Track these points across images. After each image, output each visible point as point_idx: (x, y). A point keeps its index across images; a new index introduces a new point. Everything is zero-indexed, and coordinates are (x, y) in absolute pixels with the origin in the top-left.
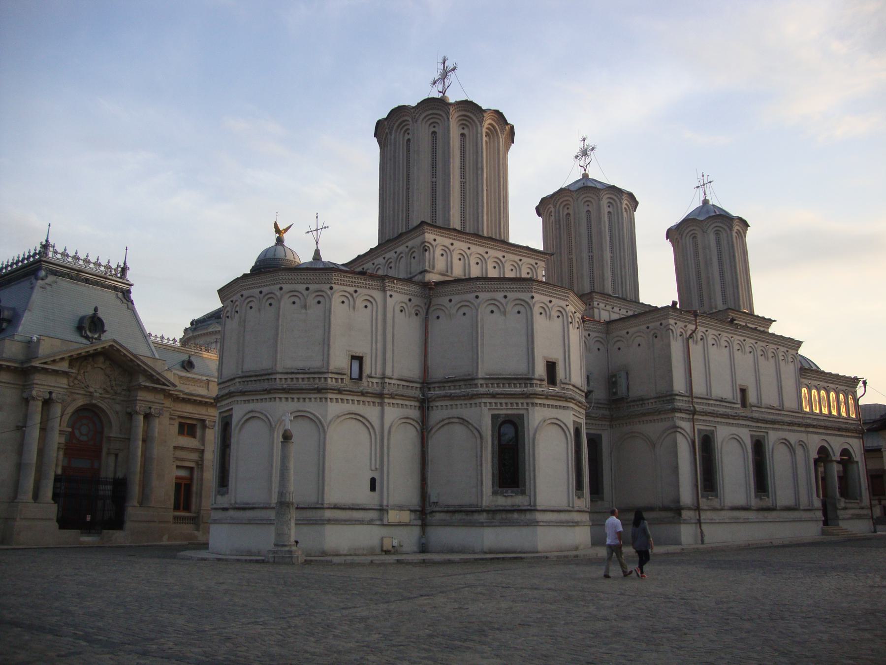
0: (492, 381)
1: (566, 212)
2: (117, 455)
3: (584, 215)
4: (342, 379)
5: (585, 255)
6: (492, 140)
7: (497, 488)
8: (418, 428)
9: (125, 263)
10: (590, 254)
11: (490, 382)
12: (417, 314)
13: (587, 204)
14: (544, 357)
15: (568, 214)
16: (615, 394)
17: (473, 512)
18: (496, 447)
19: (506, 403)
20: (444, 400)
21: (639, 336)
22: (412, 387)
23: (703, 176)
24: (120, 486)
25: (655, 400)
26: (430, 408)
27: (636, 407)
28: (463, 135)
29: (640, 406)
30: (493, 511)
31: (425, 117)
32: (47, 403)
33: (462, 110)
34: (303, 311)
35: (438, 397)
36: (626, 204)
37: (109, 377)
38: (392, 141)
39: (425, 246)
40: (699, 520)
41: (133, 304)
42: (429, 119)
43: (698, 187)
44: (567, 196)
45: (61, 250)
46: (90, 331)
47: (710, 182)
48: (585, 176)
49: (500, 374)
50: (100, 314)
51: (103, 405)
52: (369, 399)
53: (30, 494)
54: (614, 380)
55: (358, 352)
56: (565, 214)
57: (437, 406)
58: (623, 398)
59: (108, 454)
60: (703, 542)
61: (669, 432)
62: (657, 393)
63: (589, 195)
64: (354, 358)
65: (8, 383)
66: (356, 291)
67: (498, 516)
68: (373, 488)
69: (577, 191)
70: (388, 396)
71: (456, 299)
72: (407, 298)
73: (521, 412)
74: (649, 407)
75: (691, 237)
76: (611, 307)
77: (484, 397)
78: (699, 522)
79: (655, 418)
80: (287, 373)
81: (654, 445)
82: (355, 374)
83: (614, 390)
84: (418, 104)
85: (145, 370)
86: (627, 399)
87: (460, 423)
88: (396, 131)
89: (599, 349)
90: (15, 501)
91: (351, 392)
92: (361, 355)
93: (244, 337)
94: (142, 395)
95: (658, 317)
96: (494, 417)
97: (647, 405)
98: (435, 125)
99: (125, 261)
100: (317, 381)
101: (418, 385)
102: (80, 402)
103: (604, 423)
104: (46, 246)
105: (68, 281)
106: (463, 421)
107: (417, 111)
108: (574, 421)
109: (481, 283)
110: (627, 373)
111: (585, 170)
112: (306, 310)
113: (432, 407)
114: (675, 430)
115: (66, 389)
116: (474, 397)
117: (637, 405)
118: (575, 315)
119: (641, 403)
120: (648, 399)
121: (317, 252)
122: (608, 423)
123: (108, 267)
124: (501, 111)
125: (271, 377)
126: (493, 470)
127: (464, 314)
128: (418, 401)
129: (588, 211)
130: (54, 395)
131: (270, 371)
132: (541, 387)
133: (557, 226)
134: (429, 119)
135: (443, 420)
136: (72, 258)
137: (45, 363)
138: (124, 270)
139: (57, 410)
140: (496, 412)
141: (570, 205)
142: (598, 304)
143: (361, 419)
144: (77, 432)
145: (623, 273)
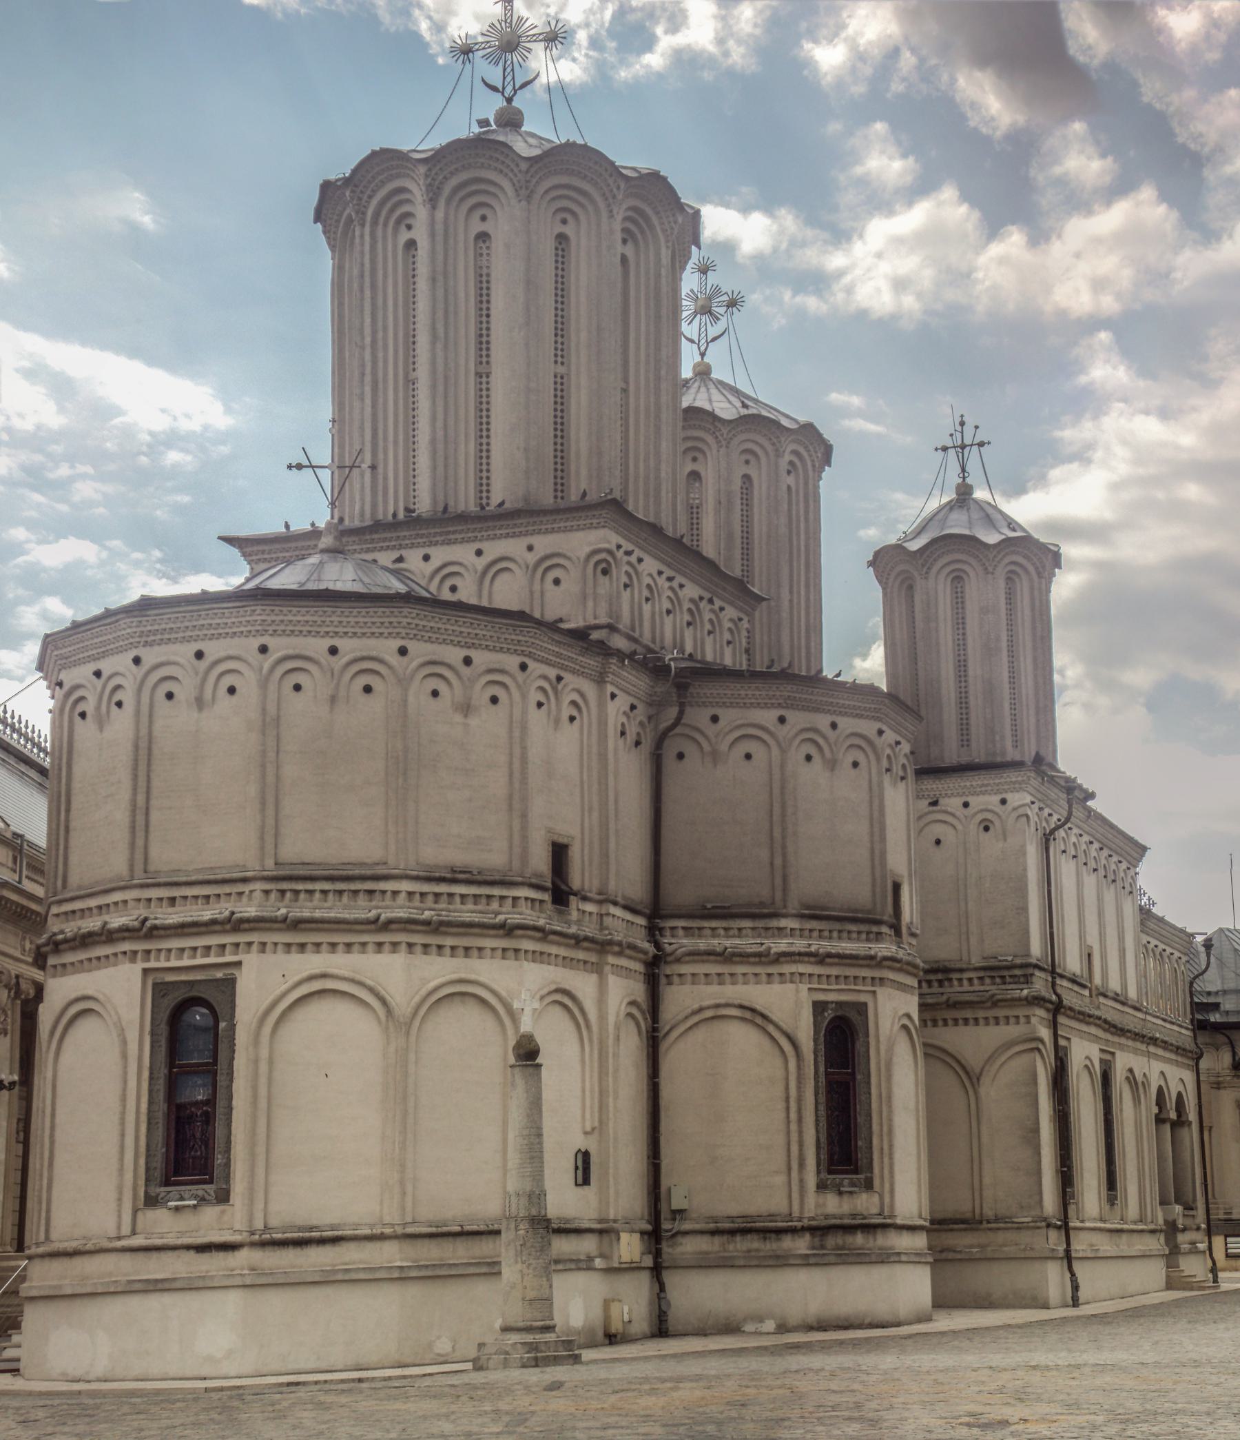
7: (824, 1175)
17: (779, 1232)
20: (707, 961)
23: (962, 424)
25: (981, 974)
29: (936, 984)
30: (821, 1230)
34: (458, 718)
40: (1068, 1252)
43: (945, 449)
47: (981, 444)
57: (680, 975)
60: (1075, 1303)
61: (1017, 1049)
63: (752, 436)
67: (831, 1241)
73: (862, 998)
75: (949, 580)
78: (1068, 1257)
80: (429, 879)
87: (743, 1019)
93: (278, 768)
96: (819, 1007)
100: (495, 905)
106: (755, 1016)
112: (466, 716)
113: (667, 976)
114: (1033, 1045)
116: (782, 959)
119: (940, 976)
120: (961, 970)
125: (382, 885)
127: (748, 756)
129: (747, 478)
131: (381, 871)
135: (701, 1010)
140: (821, 997)
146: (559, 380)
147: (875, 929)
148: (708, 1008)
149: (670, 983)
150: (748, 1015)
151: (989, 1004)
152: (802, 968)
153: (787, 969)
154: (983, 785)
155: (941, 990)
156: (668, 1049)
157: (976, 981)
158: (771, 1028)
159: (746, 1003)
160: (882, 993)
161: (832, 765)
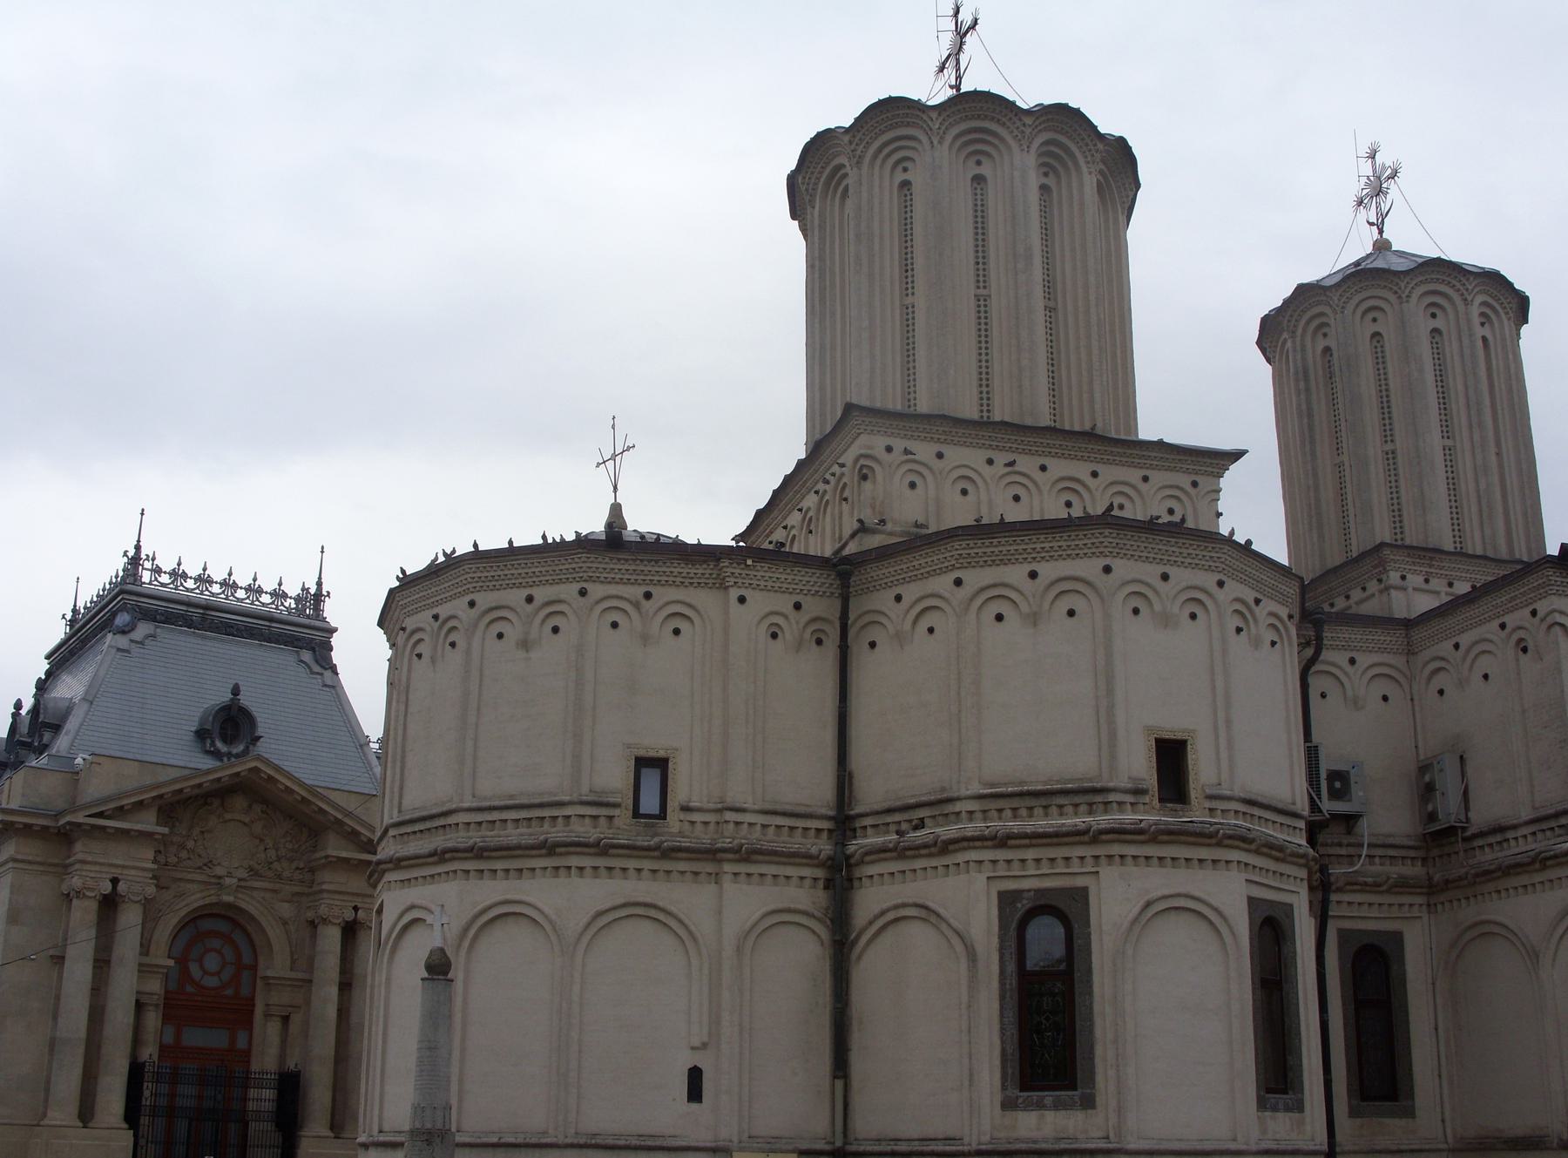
0: (1001, 803)
1: (1321, 344)
2: (286, 1019)
3: (1365, 348)
4: (611, 818)
5: (1374, 448)
6: (1064, 184)
8: (824, 934)
9: (319, 584)
10: (1389, 447)
11: (992, 805)
12: (819, 642)
13: (1370, 316)
14: (1149, 729)
15: (1327, 350)
16: (1432, 817)
18: (1013, 981)
19: (1038, 861)
21: (1484, 652)
22: (806, 829)
24: (290, 1086)
26: (856, 883)
27: (1486, 849)
28: (979, 179)
31: (880, 150)
32: (109, 904)
33: (962, 120)
35: (867, 854)
36: (1484, 304)
37: (262, 840)
38: (816, 222)
39: (862, 467)
41: (337, 674)
42: (889, 155)
44: (1319, 303)
45: (167, 565)
46: (225, 741)
48: (1382, 246)
49: (1022, 783)
50: (245, 700)
51: (249, 904)
52: (682, 866)
53: (73, 1108)
54: (1427, 778)
55: (654, 745)
56: (1320, 348)
58: (1451, 831)
59: (267, 1016)
62: (1534, 808)
64: (642, 763)
65: (30, 862)
66: (648, 596)
68: (695, 1093)
69: (1338, 285)
70: (730, 856)
71: (911, 592)
72: (784, 603)
73: (1079, 882)
74: (1517, 850)
76: (1445, 582)
77: (975, 848)
79: (1537, 878)
81: (1533, 955)
82: (650, 803)
83: (1430, 808)
84: (857, 120)
85: (339, 822)
86: (1464, 829)
88: (824, 197)
89: (1385, 698)
90: (42, 1123)
91: (633, 850)
92: (662, 754)
94: (331, 880)
95: (1523, 594)
96: (1007, 900)
97: (1513, 843)
98: (906, 164)
99: (320, 578)
100: (546, 826)
101: (826, 825)
102: (196, 898)
103: (1406, 899)
104: (135, 561)
105: (182, 632)
106: (928, 913)
107: (856, 140)
108: (1252, 901)
109: (964, 544)
110: (1461, 757)
111: (1381, 232)
112: (527, 651)
113: (861, 879)
115: (152, 870)
116: (951, 847)
117: (1491, 845)
118: (1257, 610)
120: (1515, 827)
121: (616, 509)
122: (1419, 900)
123: (278, 595)
124: (1073, 105)
126: (1003, 1042)
127: (931, 630)
128: (821, 865)
130: (122, 887)
132: (1134, 812)
133: (1302, 384)
134: (889, 155)
135: (883, 913)
136: (196, 580)
137: (100, 815)
138: (318, 598)
139: (130, 919)
141: (1327, 325)
142: (1403, 578)
143: (661, 917)
144: (194, 970)
145: (1483, 486)
146: (982, 303)
147: (1099, 798)
148: (888, 910)
149: (861, 887)
150: (923, 913)
151: (1537, 866)
152: (973, 855)
153: (960, 857)
154: (1513, 599)
155: (1499, 855)
156: (859, 957)
157: (1530, 838)
158: (944, 927)
159: (920, 901)
160: (1108, 873)
161: (1034, 619)
